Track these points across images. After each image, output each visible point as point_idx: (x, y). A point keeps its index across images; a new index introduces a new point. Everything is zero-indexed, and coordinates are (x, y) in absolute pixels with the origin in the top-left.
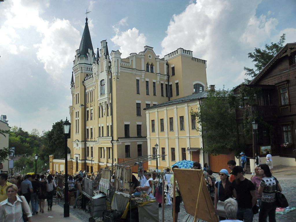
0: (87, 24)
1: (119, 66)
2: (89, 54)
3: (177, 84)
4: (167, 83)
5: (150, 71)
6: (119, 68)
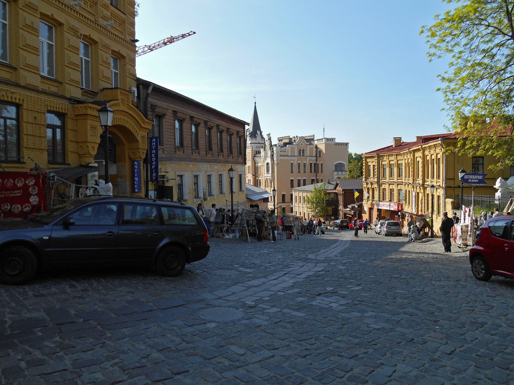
0: (255, 107)
1: (279, 156)
2: (257, 134)
3: (322, 164)
4: (315, 162)
5: (302, 155)
6: (279, 157)
